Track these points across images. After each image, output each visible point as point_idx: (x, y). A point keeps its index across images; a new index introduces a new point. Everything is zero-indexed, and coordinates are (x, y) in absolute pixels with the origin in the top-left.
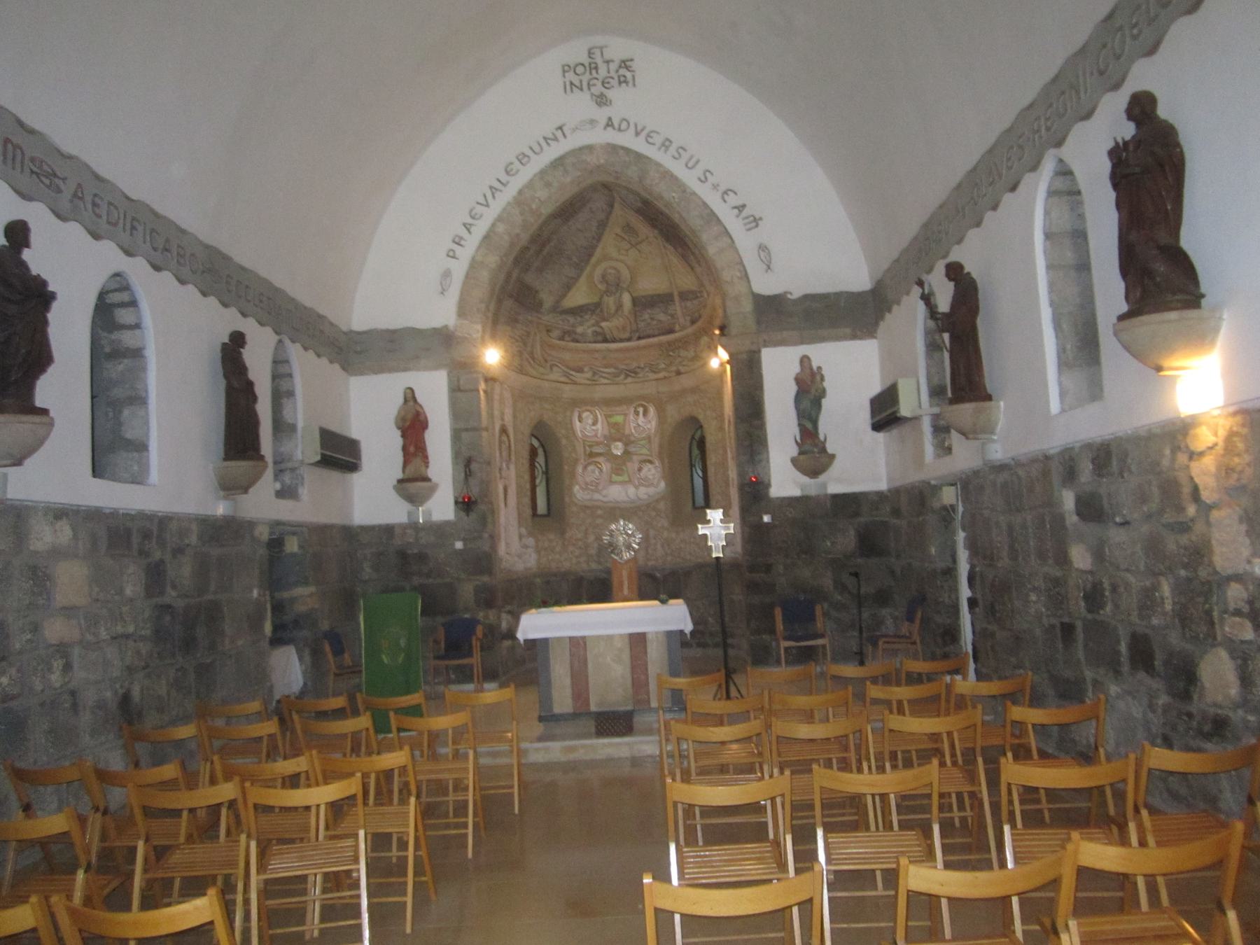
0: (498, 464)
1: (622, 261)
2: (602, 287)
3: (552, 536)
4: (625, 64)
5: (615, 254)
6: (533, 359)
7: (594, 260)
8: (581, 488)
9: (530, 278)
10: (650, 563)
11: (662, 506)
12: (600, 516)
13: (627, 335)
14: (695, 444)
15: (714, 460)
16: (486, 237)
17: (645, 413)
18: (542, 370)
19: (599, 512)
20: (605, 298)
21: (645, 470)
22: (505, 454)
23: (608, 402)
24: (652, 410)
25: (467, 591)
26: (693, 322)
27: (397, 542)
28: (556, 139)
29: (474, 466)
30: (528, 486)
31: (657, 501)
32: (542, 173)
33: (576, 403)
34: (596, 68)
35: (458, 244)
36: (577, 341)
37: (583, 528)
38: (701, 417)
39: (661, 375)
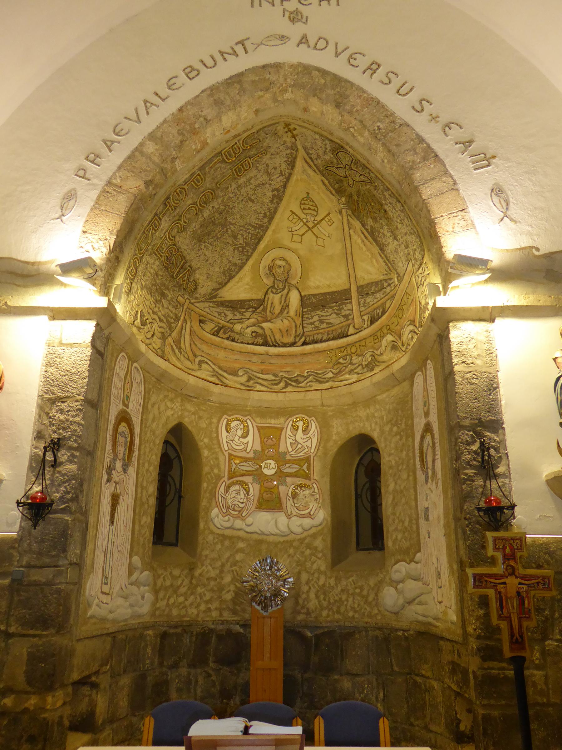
0: (108, 460)
1: (294, 251)
2: (268, 282)
3: (176, 572)
5: (287, 242)
6: (179, 349)
7: (262, 245)
8: (220, 510)
9: (184, 242)
10: (301, 617)
11: (318, 543)
12: (241, 550)
13: (291, 340)
14: (362, 470)
15: (392, 486)
18: (188, 363)
19: (241, 545)
20: (271, 295)
22: (121, 450)
23: (263, 412)
24: (314, 427)
26: (372, 322)
28: (235, 54)
29: (63, 455)
30: (153, 501)
31: (314, 536)
32: (212, 90)
33: (225, 409)
35: (92, 162)
36: (233, 340)
37: (218, 564)
38: (375, 435)
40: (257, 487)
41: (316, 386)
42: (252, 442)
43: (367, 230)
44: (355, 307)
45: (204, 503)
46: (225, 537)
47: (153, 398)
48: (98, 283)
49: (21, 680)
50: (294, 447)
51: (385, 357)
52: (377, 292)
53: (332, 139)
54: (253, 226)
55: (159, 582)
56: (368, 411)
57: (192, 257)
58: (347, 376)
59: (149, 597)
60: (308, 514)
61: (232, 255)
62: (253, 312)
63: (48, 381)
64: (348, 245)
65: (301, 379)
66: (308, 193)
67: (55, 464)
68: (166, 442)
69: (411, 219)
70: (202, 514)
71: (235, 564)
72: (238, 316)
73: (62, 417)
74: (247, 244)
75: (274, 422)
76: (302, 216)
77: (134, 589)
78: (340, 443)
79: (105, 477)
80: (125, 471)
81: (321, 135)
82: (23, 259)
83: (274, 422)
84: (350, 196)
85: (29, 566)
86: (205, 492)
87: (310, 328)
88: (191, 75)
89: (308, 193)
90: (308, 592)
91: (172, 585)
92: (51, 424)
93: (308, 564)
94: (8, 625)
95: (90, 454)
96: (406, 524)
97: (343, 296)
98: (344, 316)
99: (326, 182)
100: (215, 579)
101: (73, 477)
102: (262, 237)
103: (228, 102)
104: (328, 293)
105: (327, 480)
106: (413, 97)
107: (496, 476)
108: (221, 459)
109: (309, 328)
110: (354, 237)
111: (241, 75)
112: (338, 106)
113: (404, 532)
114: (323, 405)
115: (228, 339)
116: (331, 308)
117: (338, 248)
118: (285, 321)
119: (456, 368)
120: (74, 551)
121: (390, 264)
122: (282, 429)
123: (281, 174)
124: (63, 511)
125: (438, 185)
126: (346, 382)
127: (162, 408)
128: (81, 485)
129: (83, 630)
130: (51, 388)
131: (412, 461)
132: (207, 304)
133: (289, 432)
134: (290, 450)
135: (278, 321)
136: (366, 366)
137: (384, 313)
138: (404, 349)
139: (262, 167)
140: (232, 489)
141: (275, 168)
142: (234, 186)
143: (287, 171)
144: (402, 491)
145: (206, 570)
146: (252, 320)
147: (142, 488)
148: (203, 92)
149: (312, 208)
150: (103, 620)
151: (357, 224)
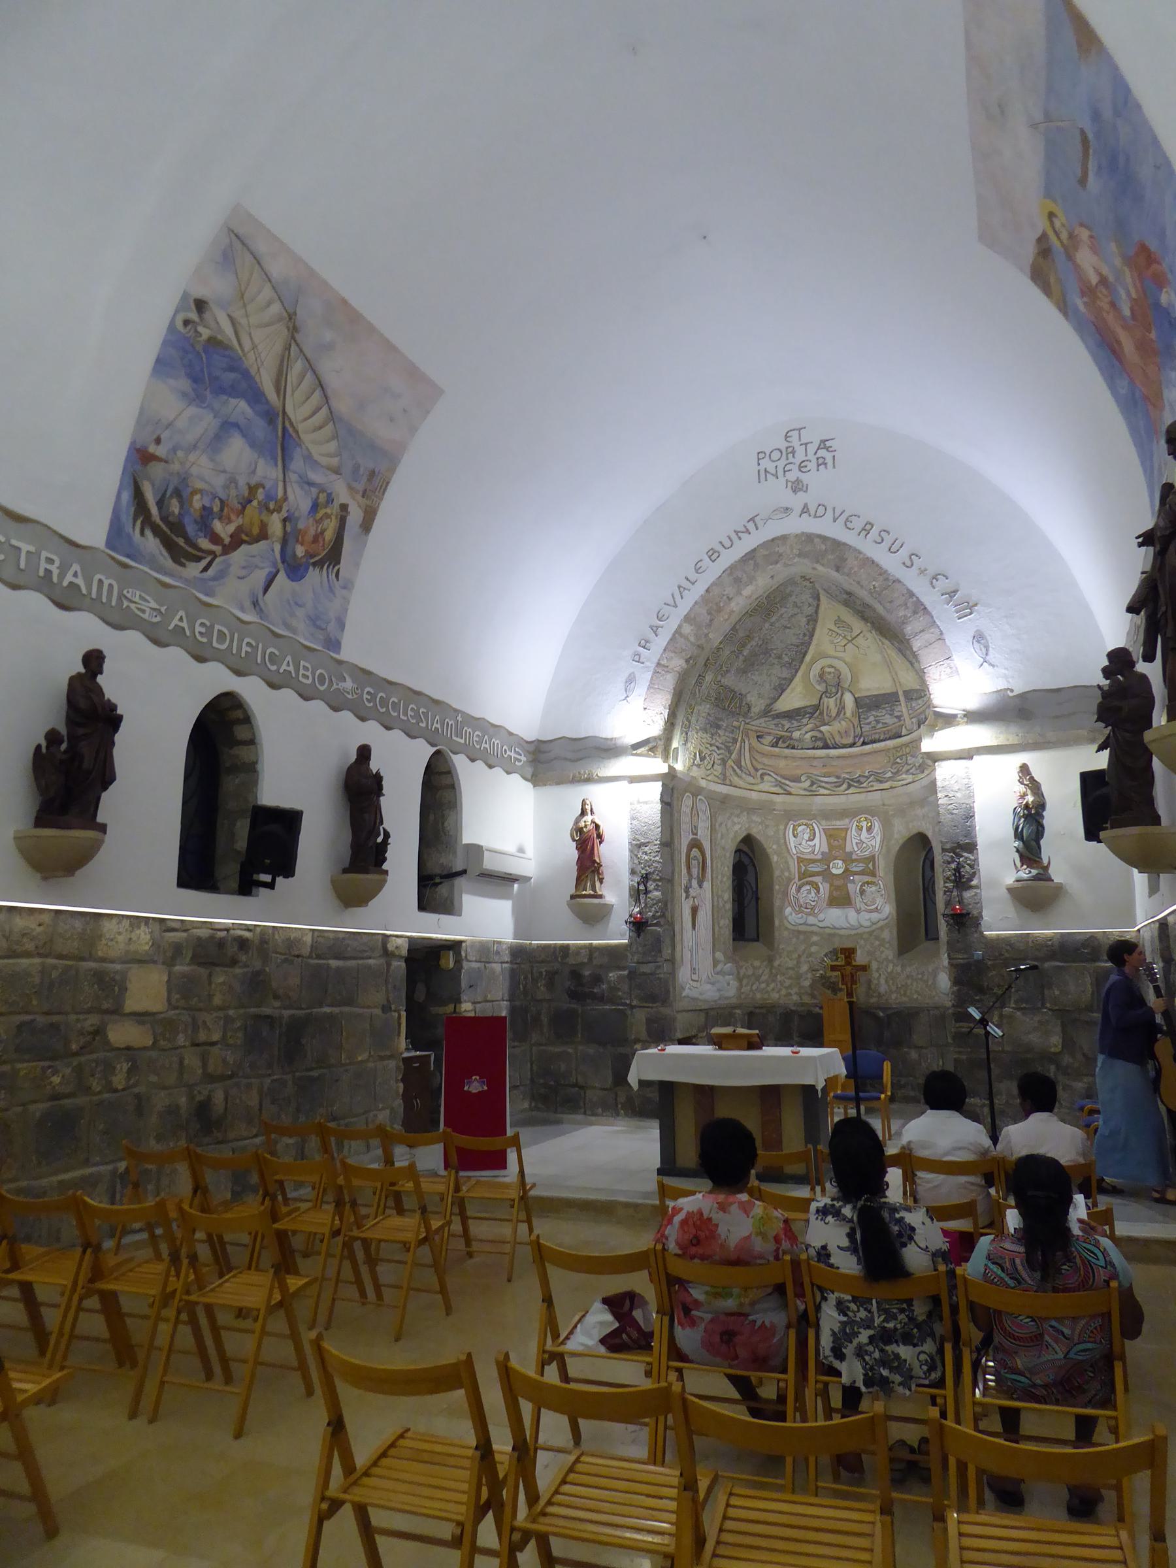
0: (684, 882)
2: (821, 688)
3: (757, 963)
4: (823, 444)
5: (832, 652)
6: (740, 767)
7: (808, 658)
8: (794, 909)
9: (729, 680)
10: (873, 1000)
11: (886, 935)
12: (814, 944)
13: (851, 740)
17: (869, 829)
18: (751, 779)
19: (815, 938)
20: (825, 700)
22: (695, 871)
25: (639, 1019)
27: (571, 960)
29: (651, 886)
30: (729, 906)
31: (881, 928)
32: (732, 569)
33: (790, 815)
34: (793, 452)
36: (793, 748)
38: (930, 835)
39: (886, 785)
40: (827, 886)
41: (877, 786)
42: (820, 844)
44: (904, 710)
45: (777, 903)
46: (799, 932)
47: (720, 819)
48: (660, 750)
49: (644, 1035)
55: (742, 972)
57: (740, 686)
59: (734, 984)
60: (872, 911)
61: (779, 672)
63: (634, 831)
65: (862, 780)
67: (646, 892)
68: (738, 851)
71: (810, 955)
72: (796, 724)
75: (839, 824)
77: (720, 977)
78: (901, 842)
79: (684, 895)
80: (701, 887)
82: (604, 736)
83: (839, 824)
85: (638, 963)
88: (713, 557)
90: (879, 978)
93: (878, 953)
94: (631, 1000)
95: (671, 881)
98: (897, 717)
100: (793, 969)
101: (659, 901)
103: (745, 579)
105: (891, 878)
106: (903, 553)
107: (972, 887)
109: (866, 728)
111: (754, 550)
112: (837, 571)
115: (787, 747)
120: (666, 952)
122: (847, 829)
124: (656, 925)
125: (927, 636)
127: (729, 823)
128: (666, 905)
129: (680, 1005)
132: (762, 720)
133: (854, 832)
143: (815, 603)
145: (784, 961)
146: (810, 726)
147: (718, 897)
150: (695, 999)
151: (887, 642)
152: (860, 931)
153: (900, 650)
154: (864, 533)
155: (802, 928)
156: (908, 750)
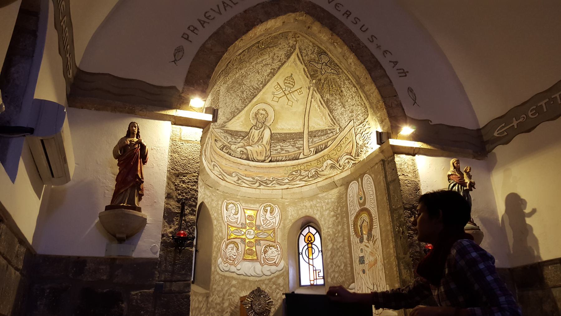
2: (254, 122)
5: (269, 101)
7: (255, 100)
12: (234, 286)
13: (263, 158)
16: (216, 33)
19: (234, 282)
21: (270, 252)
24: (277, 211)
26: (316, 153)
31: (278, 277)
33: (226, 196)
35: (193, 31)
36: (230, 155)
37: (221, 294)
38: (317, 217)
43: (324, 101)
46: (226, 277)
50: (265, 222)
51: (325, 173)
52: (323, 135)
53: (320, 46)
54: (253, 88)
56: (311, 203)
58: (298, 182)
61: (238, 103)
62: (242, 139)
63: (173, 161)
64: (308, 108)
66: (292, 74)
69: (361, 97)
70: (213, 261)
71: (230, 294)
72: (234, 140)
73: (184, 186)
74: (247, 98)
76: (283, 87)
81: (313, 44)
84: (320, 80)
86: (215, 247)
87: (275, 152)
89: (292, 74)
91: (198, 307)
92: (176, 189)
93: (275, 294)
96: (342, 267)
97: (300, 136)
99: (306, 70)
102: (256, 95)
104: (288, 134)
105: (286, 243)
108: (223, 226)
110: (314, 103)
113: (340, 273)
114: (282, 198)
115: (227, 153)
116: (289, 142)
117: (301, 108)
118: (260, 146)
119: (400, 177)
121: (334, 120)
122: (258, 211)
123: (280, 61)
126: (298, 186)
130: (176, 167)
131: (346, 231)
132: (219, 130)
133: (262, 213)
134: (263, 224)
135: (256, 146)
136: (311, 177)
137: (326, 147)
138: (341, 168)
139: (271, 54)
140: (229, 246)
141: (278, 57)
142: (255, 62)
143: (284, 60)
144: (338, 249)
145: (215, 298)
146: (241, 144)
148: (258, 5)
149: (291, 83)
151: (318, 96)
152: (264, 277)
153: (327, 103)
154: (346, 15)
155: (227, 274)
156: (302, 167)
